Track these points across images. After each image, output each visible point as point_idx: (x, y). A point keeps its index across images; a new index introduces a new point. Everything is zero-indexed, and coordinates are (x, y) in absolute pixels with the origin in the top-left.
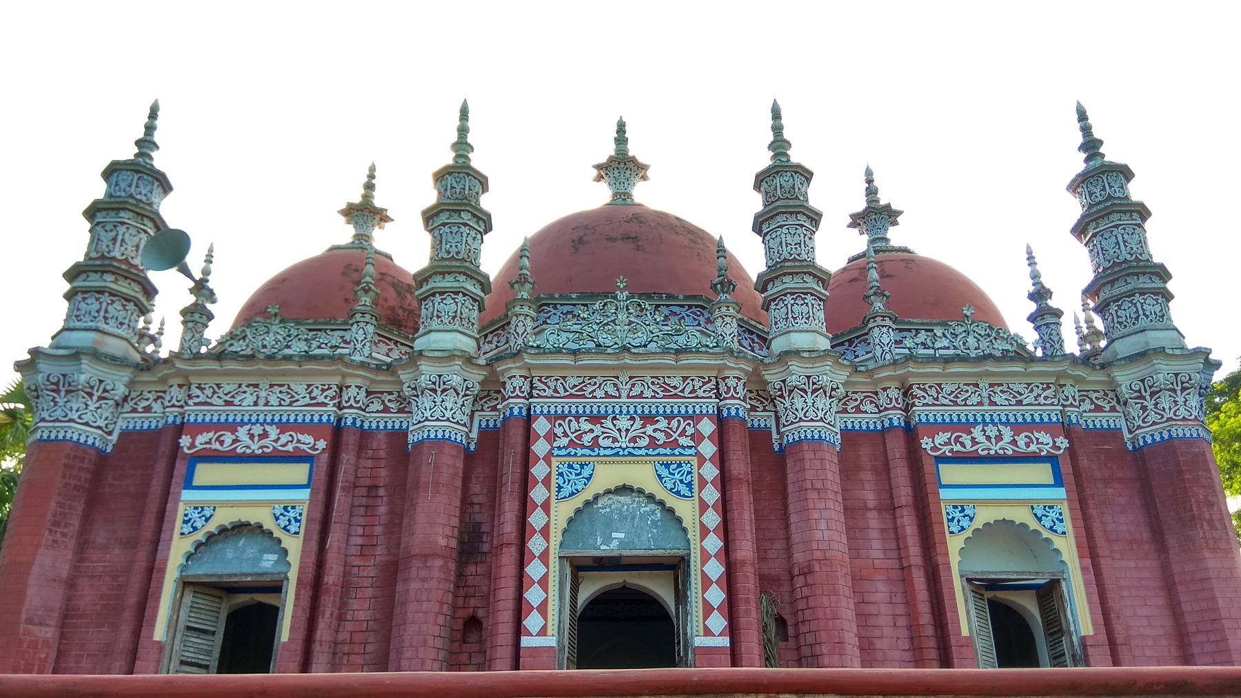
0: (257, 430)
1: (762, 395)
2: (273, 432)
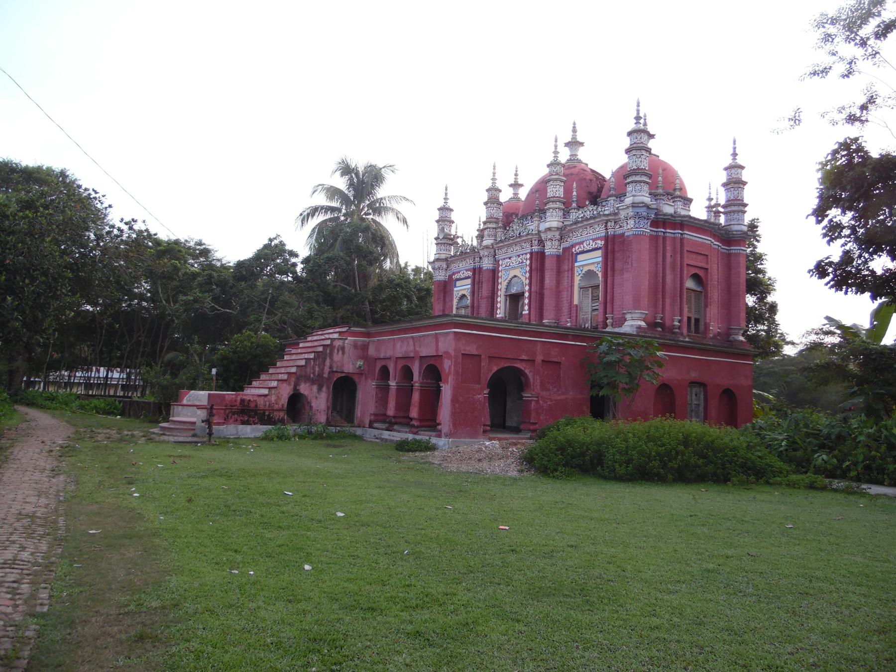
1: (541, 242)
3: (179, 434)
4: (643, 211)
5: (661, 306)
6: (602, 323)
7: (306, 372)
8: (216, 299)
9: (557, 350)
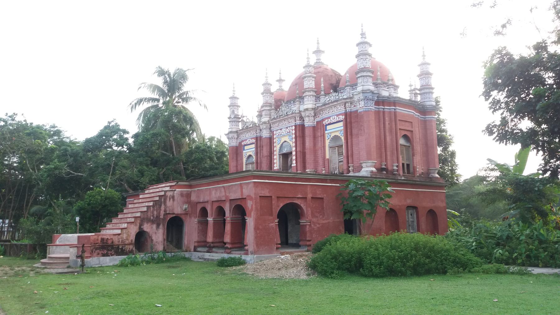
1: (302, 118)
2: (250, 139)
3: (57, 267)
4: (370, 96)
5: (384, 157)
6: (346, 170)
7: (147, 216)
8: (70, 166)
9: (320, 190)
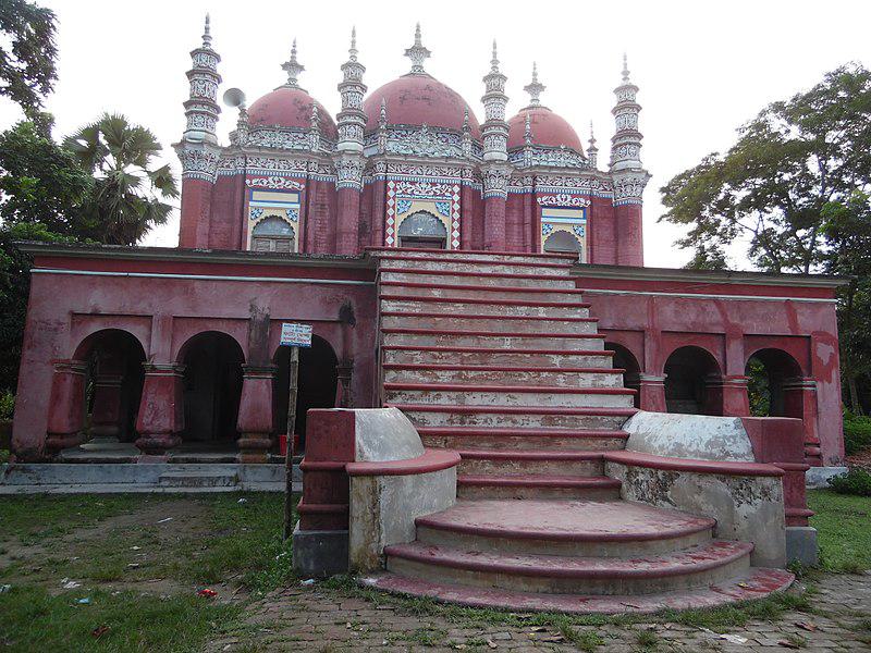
0: (276, 179)
